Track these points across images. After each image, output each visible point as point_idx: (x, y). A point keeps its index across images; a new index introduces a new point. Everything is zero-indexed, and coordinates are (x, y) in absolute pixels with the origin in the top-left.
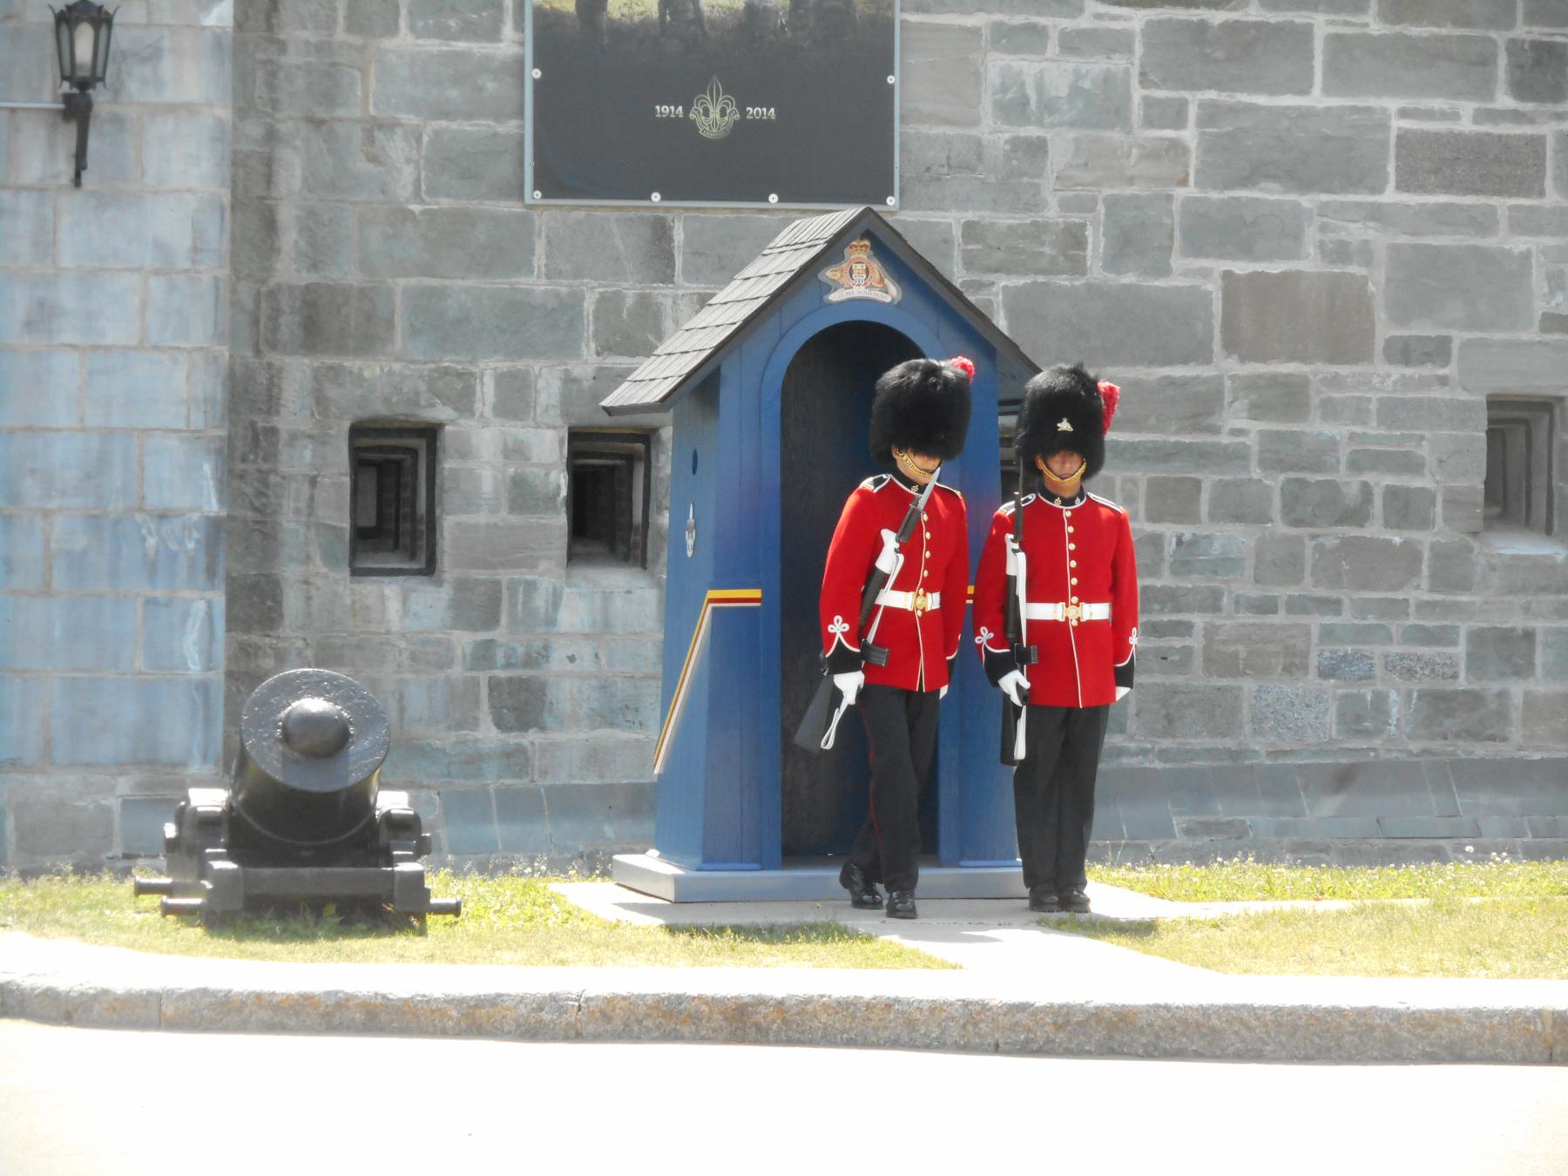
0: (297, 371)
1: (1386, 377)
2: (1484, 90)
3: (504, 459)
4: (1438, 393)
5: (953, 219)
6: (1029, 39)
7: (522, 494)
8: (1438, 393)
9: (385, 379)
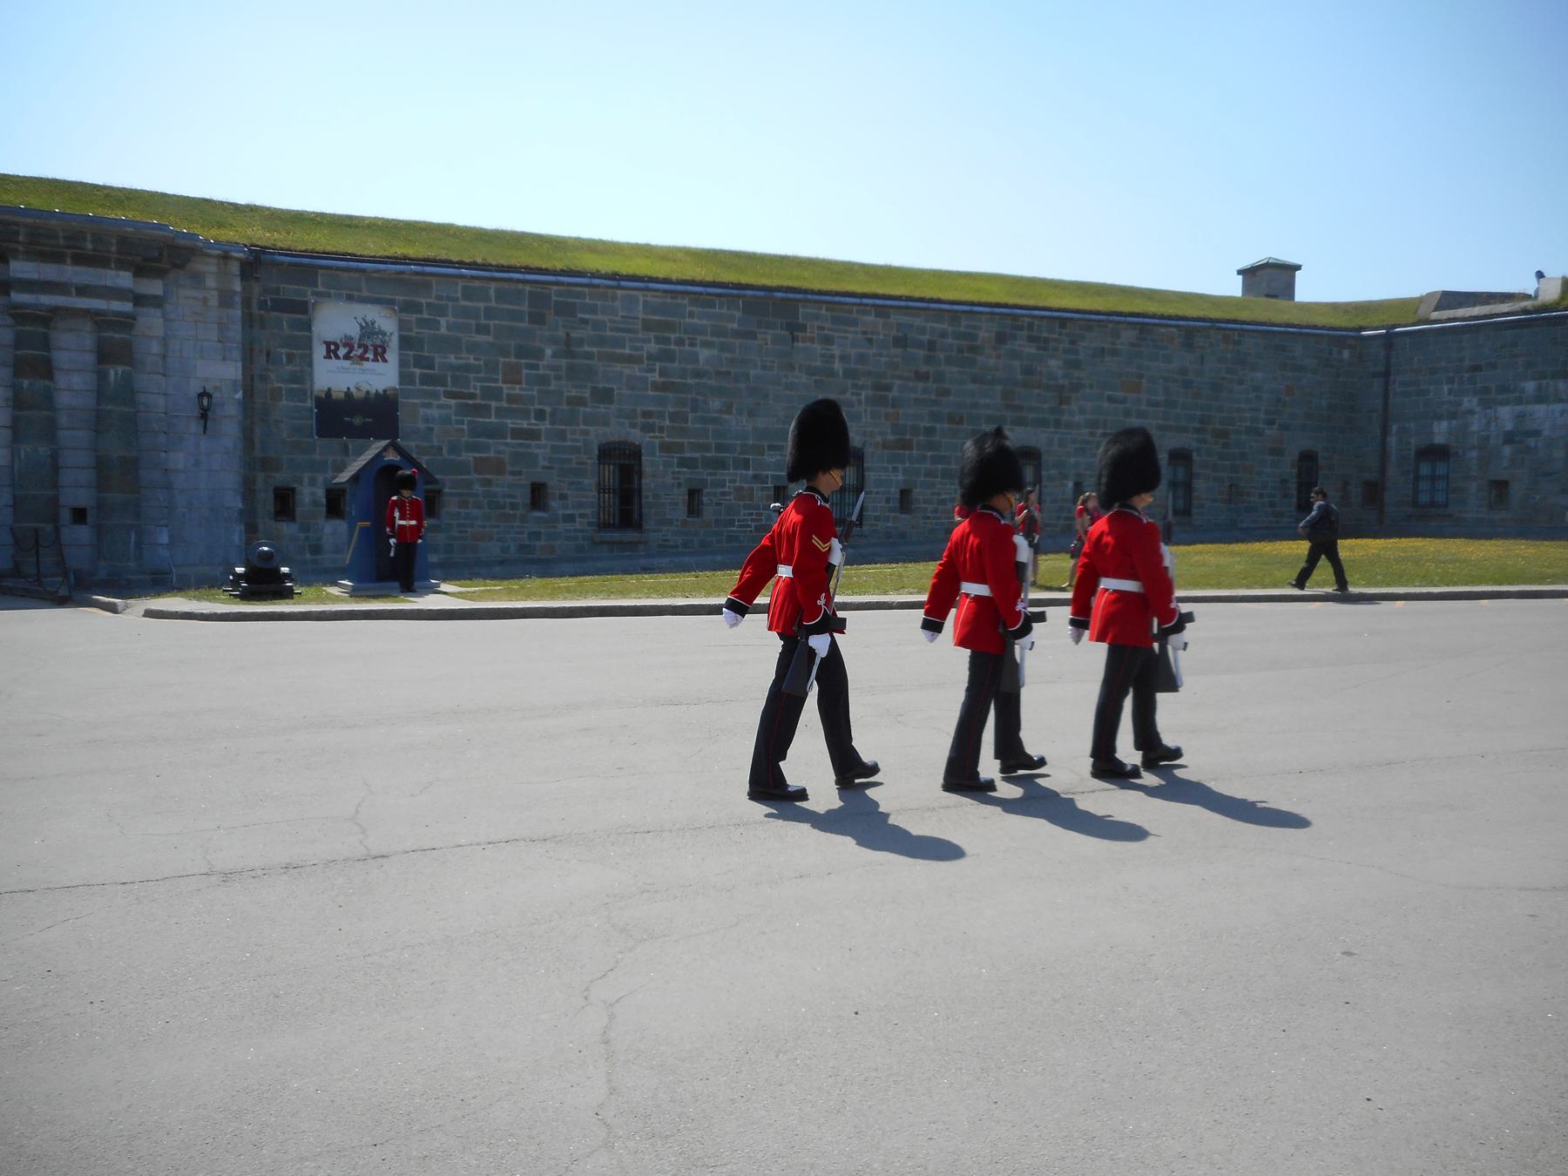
0: (260, 476)
1: (509, 478)
2: (528, 418)
3: (310, 494)
5: (413, 444)
6: (429, 406)
7: (315, 503)
9: (281, 477)
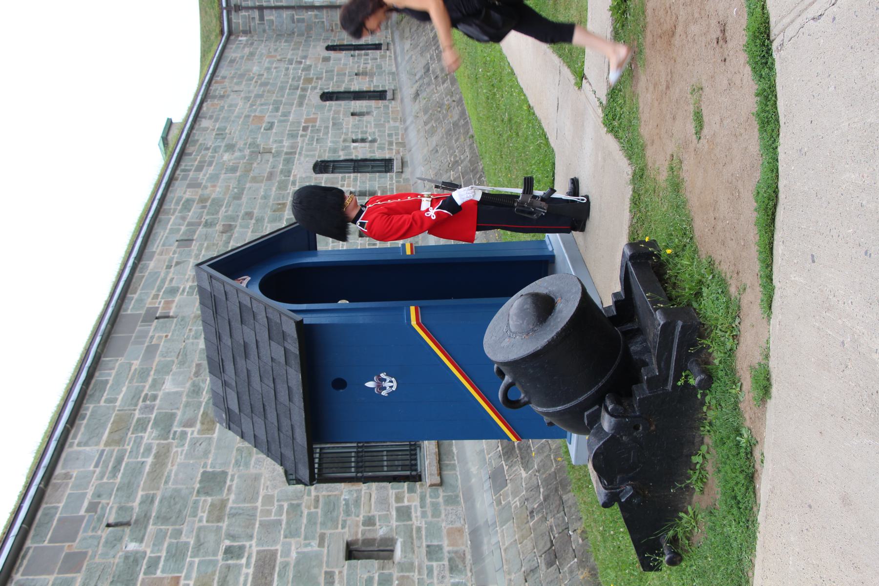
2: (239, 567)
4: (345, 572)
8: (345, 572)
